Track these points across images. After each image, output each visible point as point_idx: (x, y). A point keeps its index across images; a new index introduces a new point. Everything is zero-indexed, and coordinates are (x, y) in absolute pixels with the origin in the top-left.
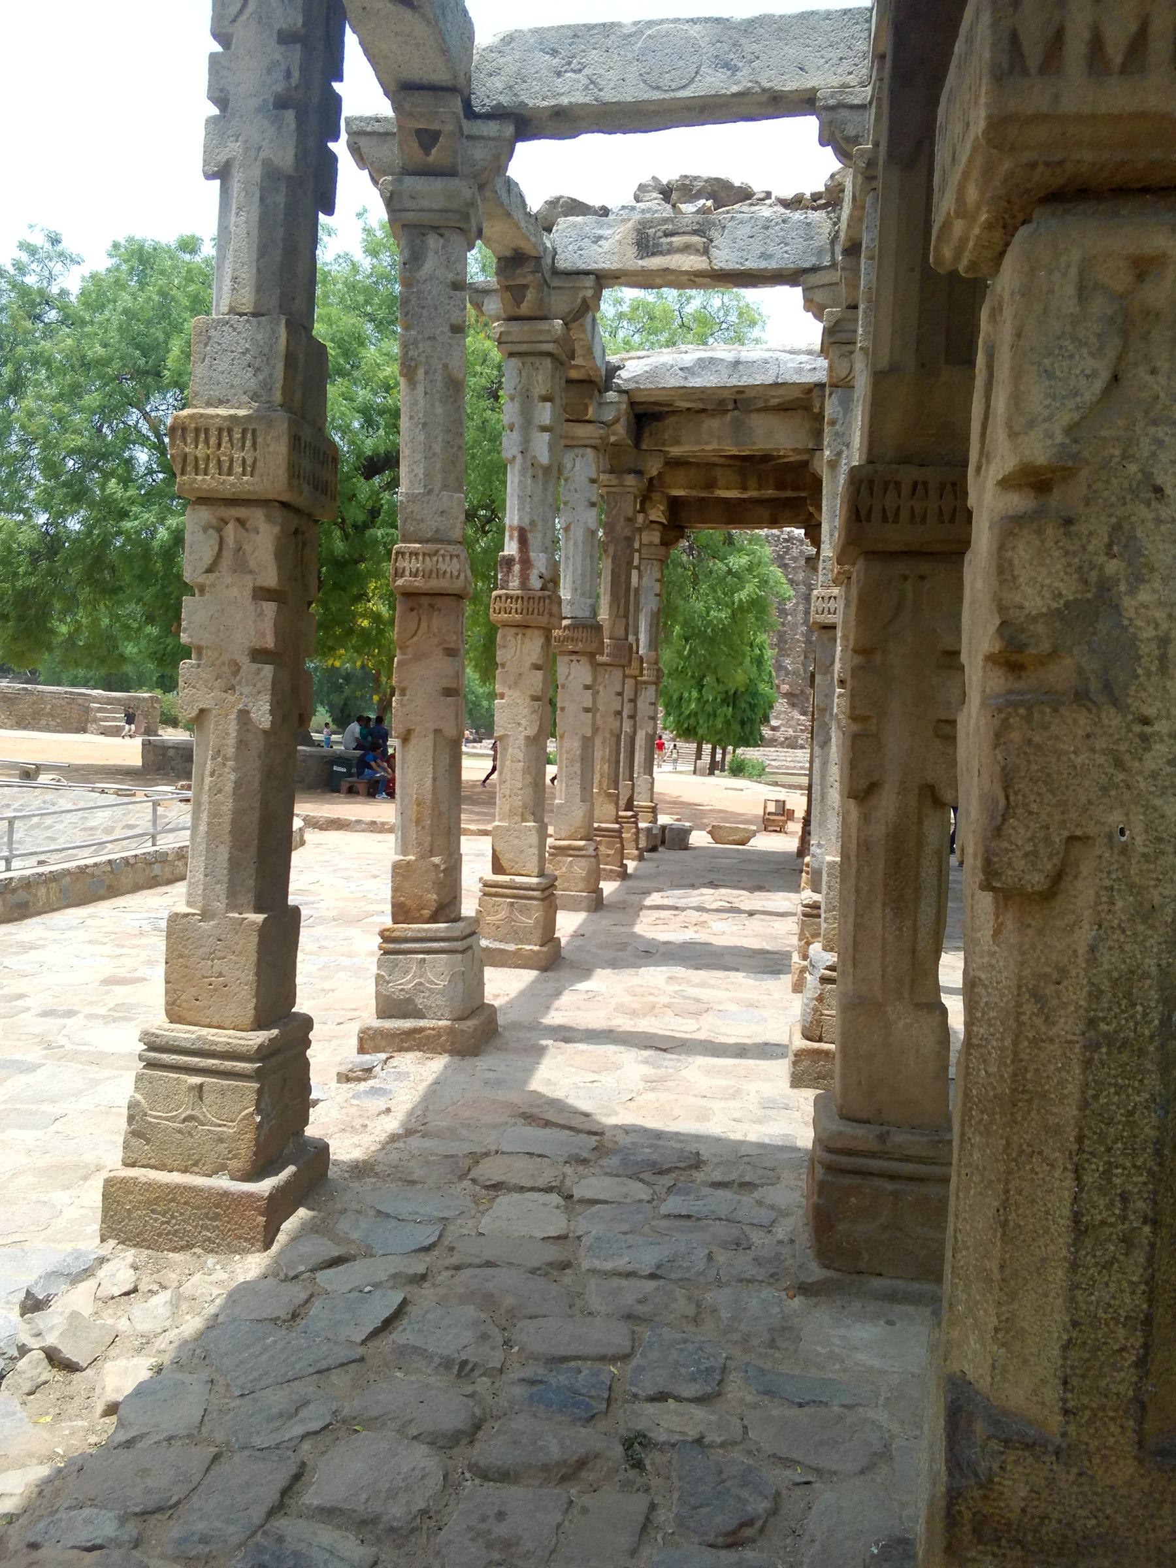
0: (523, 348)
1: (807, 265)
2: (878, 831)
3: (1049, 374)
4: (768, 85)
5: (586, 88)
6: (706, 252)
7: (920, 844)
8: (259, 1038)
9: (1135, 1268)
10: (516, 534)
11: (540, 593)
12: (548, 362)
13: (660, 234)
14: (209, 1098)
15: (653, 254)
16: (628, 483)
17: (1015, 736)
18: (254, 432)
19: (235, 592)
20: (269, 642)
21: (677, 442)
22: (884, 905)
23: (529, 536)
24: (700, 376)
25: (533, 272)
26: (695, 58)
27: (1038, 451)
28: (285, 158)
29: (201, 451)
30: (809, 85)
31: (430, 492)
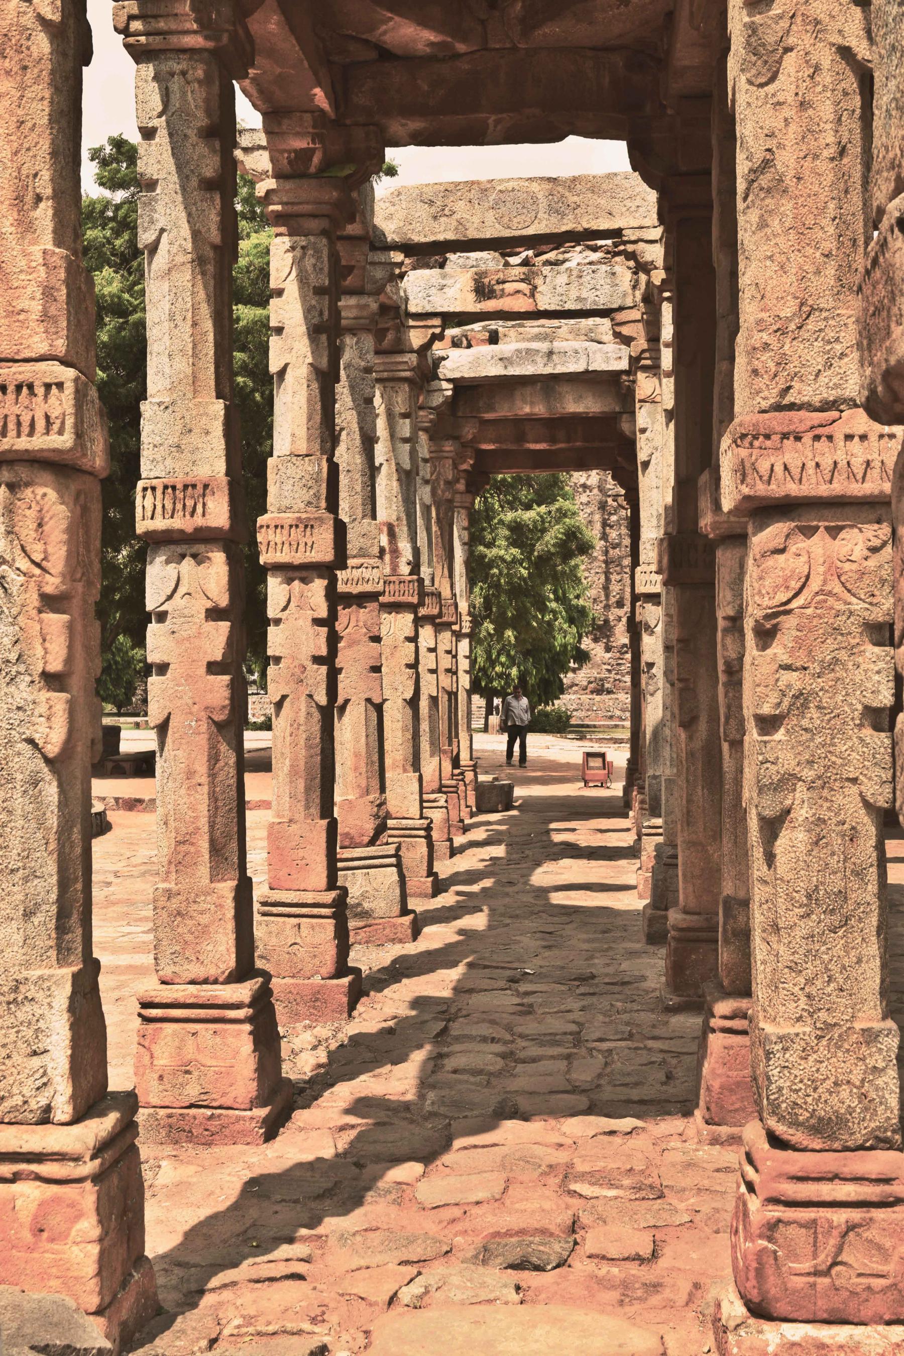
0: (385, 375)
1: (615, 306)
2: (698, 744)
3: (733, 589)
4: (586, 226)
5: (456, 229)
6: (532, 295)
10: (385, 529)
11: (409, 578)
12: (406, 387)
13: (493, 282)
14: (304, 931)
15: (489, 298)
16: (448, 449)
17: (731, 695)
18: (312, 526)
19: (301, 622)
21: (491, 409)
22: (703, 788)
23: (397, 530)
24: (519, 365)
25: (394, 319)
26: (534, 207)
27: (731, 613)
28: (324, 363)
29: (278, 539)
30: (616, 227)
31: (355, 520)
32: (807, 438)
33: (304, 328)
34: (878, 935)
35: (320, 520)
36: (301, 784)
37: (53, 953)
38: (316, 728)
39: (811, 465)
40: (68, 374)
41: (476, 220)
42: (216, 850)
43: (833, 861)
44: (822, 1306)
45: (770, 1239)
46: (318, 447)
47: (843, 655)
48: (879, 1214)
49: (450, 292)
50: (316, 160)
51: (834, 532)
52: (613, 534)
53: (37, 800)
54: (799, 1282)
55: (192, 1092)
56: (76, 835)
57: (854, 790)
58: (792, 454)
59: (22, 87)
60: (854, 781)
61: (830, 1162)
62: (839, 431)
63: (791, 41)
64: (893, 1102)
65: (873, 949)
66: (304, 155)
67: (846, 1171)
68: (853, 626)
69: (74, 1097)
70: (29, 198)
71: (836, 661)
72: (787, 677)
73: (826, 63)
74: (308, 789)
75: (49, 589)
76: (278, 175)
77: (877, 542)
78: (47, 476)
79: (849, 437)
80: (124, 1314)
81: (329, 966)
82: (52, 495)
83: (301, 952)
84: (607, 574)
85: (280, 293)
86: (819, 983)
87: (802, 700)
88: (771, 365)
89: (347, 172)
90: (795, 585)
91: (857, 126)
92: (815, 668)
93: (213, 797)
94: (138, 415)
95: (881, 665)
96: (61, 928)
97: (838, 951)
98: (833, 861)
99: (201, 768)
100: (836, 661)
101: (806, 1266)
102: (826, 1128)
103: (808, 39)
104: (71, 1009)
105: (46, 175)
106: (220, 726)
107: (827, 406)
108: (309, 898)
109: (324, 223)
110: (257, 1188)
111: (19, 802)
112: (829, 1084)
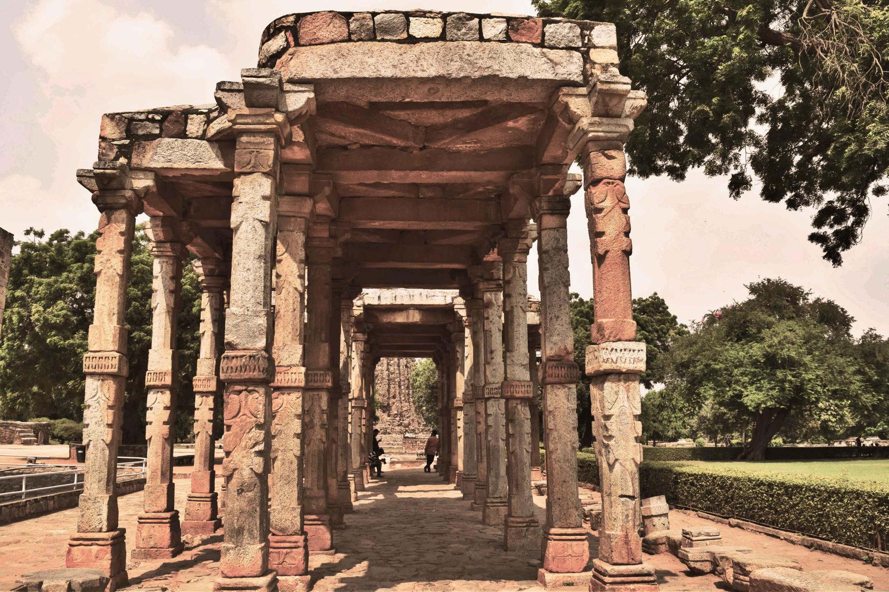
28: (216, 331)
38: (209, 442)
40: (118, 354)
42: (163, 474)
51: (289, 394)
52: (392, 369)
53: (104, 454)
55: (152, 543)
56: (113, 463)
61: (283, 538)
62: (290, 372)
65: (296, 489)
68: (292, 415)
76: (205, 275)
81: (208, 517)
83: (200, 512)
84: (389, 385)
87: (280, 432)
93: (163, 459)
94: (148, 353)
96: (108, 485)
99: (160, 451)
102: (283, 530)
104: (108, 504)
106: (166, 439)
107: (288, 366)
108: (203, 495)
110: (165, 565)
111: (99, 454)
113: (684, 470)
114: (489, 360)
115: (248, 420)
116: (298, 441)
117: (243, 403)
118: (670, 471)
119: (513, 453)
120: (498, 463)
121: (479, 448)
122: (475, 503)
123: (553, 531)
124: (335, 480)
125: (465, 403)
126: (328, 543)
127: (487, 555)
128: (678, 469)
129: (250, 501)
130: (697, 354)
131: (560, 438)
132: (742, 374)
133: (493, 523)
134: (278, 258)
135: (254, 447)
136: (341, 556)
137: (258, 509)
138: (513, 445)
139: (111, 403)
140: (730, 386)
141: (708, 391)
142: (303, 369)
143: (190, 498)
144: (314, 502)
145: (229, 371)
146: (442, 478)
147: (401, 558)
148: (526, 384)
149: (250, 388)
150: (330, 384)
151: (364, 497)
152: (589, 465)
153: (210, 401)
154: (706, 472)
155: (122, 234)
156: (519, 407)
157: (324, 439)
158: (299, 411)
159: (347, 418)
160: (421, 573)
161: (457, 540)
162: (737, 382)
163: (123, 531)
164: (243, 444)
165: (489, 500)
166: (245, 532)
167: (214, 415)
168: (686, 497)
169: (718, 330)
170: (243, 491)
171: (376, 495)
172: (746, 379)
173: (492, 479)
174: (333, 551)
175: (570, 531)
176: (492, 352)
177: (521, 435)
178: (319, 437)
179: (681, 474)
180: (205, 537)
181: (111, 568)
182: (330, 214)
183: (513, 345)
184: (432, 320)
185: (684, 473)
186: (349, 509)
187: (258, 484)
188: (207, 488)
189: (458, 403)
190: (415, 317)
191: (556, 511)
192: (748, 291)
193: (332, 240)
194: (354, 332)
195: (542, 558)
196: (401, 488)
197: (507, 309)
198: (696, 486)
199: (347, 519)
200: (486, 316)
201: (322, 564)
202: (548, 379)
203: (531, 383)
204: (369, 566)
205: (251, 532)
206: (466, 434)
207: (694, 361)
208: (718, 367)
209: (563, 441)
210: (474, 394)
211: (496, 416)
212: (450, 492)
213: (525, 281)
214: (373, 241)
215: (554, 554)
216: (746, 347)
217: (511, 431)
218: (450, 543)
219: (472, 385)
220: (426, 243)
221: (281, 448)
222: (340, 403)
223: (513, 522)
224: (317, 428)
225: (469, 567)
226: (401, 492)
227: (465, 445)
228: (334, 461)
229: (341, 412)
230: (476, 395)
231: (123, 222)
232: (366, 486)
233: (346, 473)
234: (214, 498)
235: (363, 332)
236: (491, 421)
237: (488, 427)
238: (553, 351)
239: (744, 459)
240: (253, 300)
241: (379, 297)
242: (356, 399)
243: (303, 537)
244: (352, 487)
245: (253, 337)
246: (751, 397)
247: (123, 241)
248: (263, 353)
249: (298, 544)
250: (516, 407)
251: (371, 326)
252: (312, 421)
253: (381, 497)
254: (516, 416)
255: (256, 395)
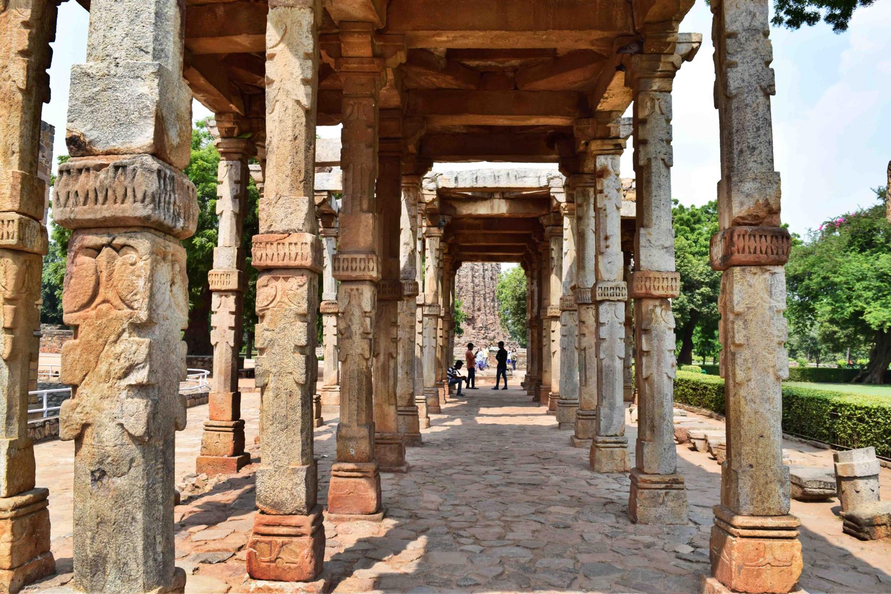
2: (380, 364)
7: (389, 367)
8: (234, 422)
9: (356, 404)
14: (221, 437)
20: (233, 325)
28: (237, 211)
32: (275, 244)
33: (229, 197)
34: (302, 432)
35: (233, 272)
36: (223, 378)
37: (4, 433)
39: (276, 254)
40: (18, 216)
41: (325, 154)
43: (282, 404)
44: (272, 576)
45: (254, 548)
46: (233, 243)
47: (288, 325)
48: (295, 539)
49: (331, 182)
50: (236, 131)
51: (286, 279)
52: (477, 281)
54: (264, 565)
57: (291, 377)
58: (271, 250)
59: (10, 112)
60: (291, 373)
62: (287, 241)
63: (278, 98)
64: (303, 496)
65: (299, 438)
66: (230, 130)
67: (284, 522)
69: (8, 488)
70: (10, 152)
71: (285, 327)
72: (268, 334)
73: (290, 106)
74: (225, 380)
75: (7, 296)
76: (223, 137)
77: (301, 283)
78: (8, 254)
79: (290, 244)
80: (29, 572)
82: (10, 261)
83: (220, 446)
84: (474, 297)
85: (222, 182)
86: (276, 450)
88: (265, 217)
89: (249, 136)
90: (270, 299)
91: (303, 129)
92: (277, 330)
95: (302, 329)
97: (283, 438)
98: (282, 404)
100: (285, 327)
101: (267, 559)
103: (284, 97)
105: (17, 144)
108: (224, 424)
109: (240, 156)
112: (279, 489)
113: (848, 400)
114: (603, 249)
115: (114, 313)
116: (302, 358)
117: (104, 276)
118: (827, 401)
119: (646, 379)
120: (614, 389)
121: (583, 368)
122: (576, 437)
123: (739, 520)
124: (393, 408)
125: (563, 311)
126: (373, 504)
127: (608, 530)
128: (836, 399)
129: (120, 499)
130: (813, 265)
131: (755, 360)
132: (866, 288)
133: (605, 469)
134: (269, 52)
135: (126, 374)
136: (390, 523)
137: (139, 516)
138: (648, 367)
139: (8, 294)
140: (850, 302)
141: (823, 307)
142: (309, 238)
143: (208, 428)
144: (352, 444)
145: (72, 200)
146: (531, 397)
147: (477, 531)
148: (670, 276)
149: (119, 241)
150: (374, 274)
151: (439, 422)
152: (705, 388)
153: (230, 302)
154: (885, 405)
155: (26, 24)
156: (658, 310)
157: (367, 355)
158: (304, 306)
159: (413, 327)
160: (509, 570)
161: (558, 497)
162: (859, 297)
163: (44, 494)
164: (103, 367)
165: (600, 439)
166: (109, 566)
167: (236, 320)
168: (850, 436)
169: (839, 239)
170: (103, 473)
171: (453, 419)
172: (870, 294)
173: (604, 411)
174: (380, 515)
175: (770, 522)
176: (606, 238)
177: (660, 352)
178: (359, 351)
179: (841, 406)
180: (224, 478)
181: (11, 554)
182: (371, 17)
183: (650, 215)
184: (521, 211)
185: (849, 405)
186: (416, 440)
187: (139, 459)
188: (229, 415)
189: (551, 312)
190: (500, 207)
191: (745, 487)
192: (877, 196)
193: (377, 61)
194: (428, 226)
195: (714, 561)
196: (483, 410)
197: (641, 163)
198: (867, 423)
199: (412, 455)
200: (599, 188)
201: (360, 541)
202: (737, 257)
203: (678, 276)
204: (428, 549)
205: (122, 568)
206: (564, 349)
207: (810, 274)
208: (837, 280)
209: (761, 365)
210: (577, 299)
211: (612, 326)
212: (541, 418)
213: (668, 120)
214: (443, 86)
215: (740, 562)
216: (871, 259)
217: (645, 347)
218: (551, 503)
219: (573, 288)
220: (516, 88)
221: (274, 370)
222: (402, 306)
223: (645, 481)
224: (357, 338)
225: (584, 558)
226: (482, 415)
227: (563, 363)
228: (391, 382)
229: (401, 319)
230: (582, 300)
231: (27, 6)
232: (443, 407)
233: (412, 396)
234: (238, 429)
235: (439, 226)
236: (604, 332)
237: (599, 340)
238: (745, 207)
239: (860, 381)
240: (128, 42)
241: (456, 179)
242: (430, 306)
243: (311, 517)
244: (422, 410)
245: (124, 123)
246: (874, 314)
247: (27, 36)
248: (149, 160)
249: (302, 530)
250: (653, 311)
251: (448, 219)
252: (349, 327)
253: (458, 422)
254: (654, 325)
255: (132, 256)
